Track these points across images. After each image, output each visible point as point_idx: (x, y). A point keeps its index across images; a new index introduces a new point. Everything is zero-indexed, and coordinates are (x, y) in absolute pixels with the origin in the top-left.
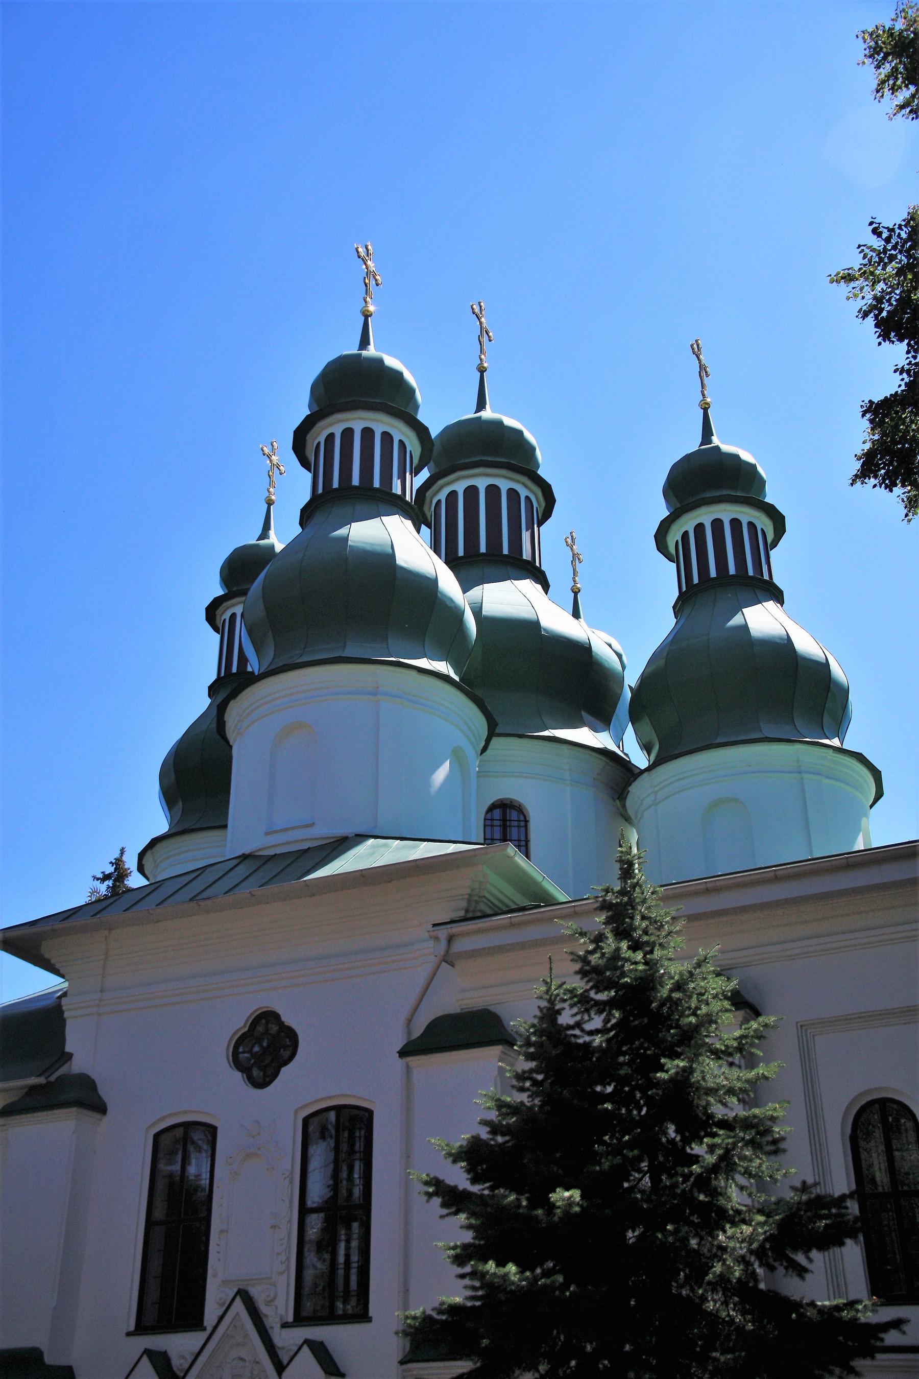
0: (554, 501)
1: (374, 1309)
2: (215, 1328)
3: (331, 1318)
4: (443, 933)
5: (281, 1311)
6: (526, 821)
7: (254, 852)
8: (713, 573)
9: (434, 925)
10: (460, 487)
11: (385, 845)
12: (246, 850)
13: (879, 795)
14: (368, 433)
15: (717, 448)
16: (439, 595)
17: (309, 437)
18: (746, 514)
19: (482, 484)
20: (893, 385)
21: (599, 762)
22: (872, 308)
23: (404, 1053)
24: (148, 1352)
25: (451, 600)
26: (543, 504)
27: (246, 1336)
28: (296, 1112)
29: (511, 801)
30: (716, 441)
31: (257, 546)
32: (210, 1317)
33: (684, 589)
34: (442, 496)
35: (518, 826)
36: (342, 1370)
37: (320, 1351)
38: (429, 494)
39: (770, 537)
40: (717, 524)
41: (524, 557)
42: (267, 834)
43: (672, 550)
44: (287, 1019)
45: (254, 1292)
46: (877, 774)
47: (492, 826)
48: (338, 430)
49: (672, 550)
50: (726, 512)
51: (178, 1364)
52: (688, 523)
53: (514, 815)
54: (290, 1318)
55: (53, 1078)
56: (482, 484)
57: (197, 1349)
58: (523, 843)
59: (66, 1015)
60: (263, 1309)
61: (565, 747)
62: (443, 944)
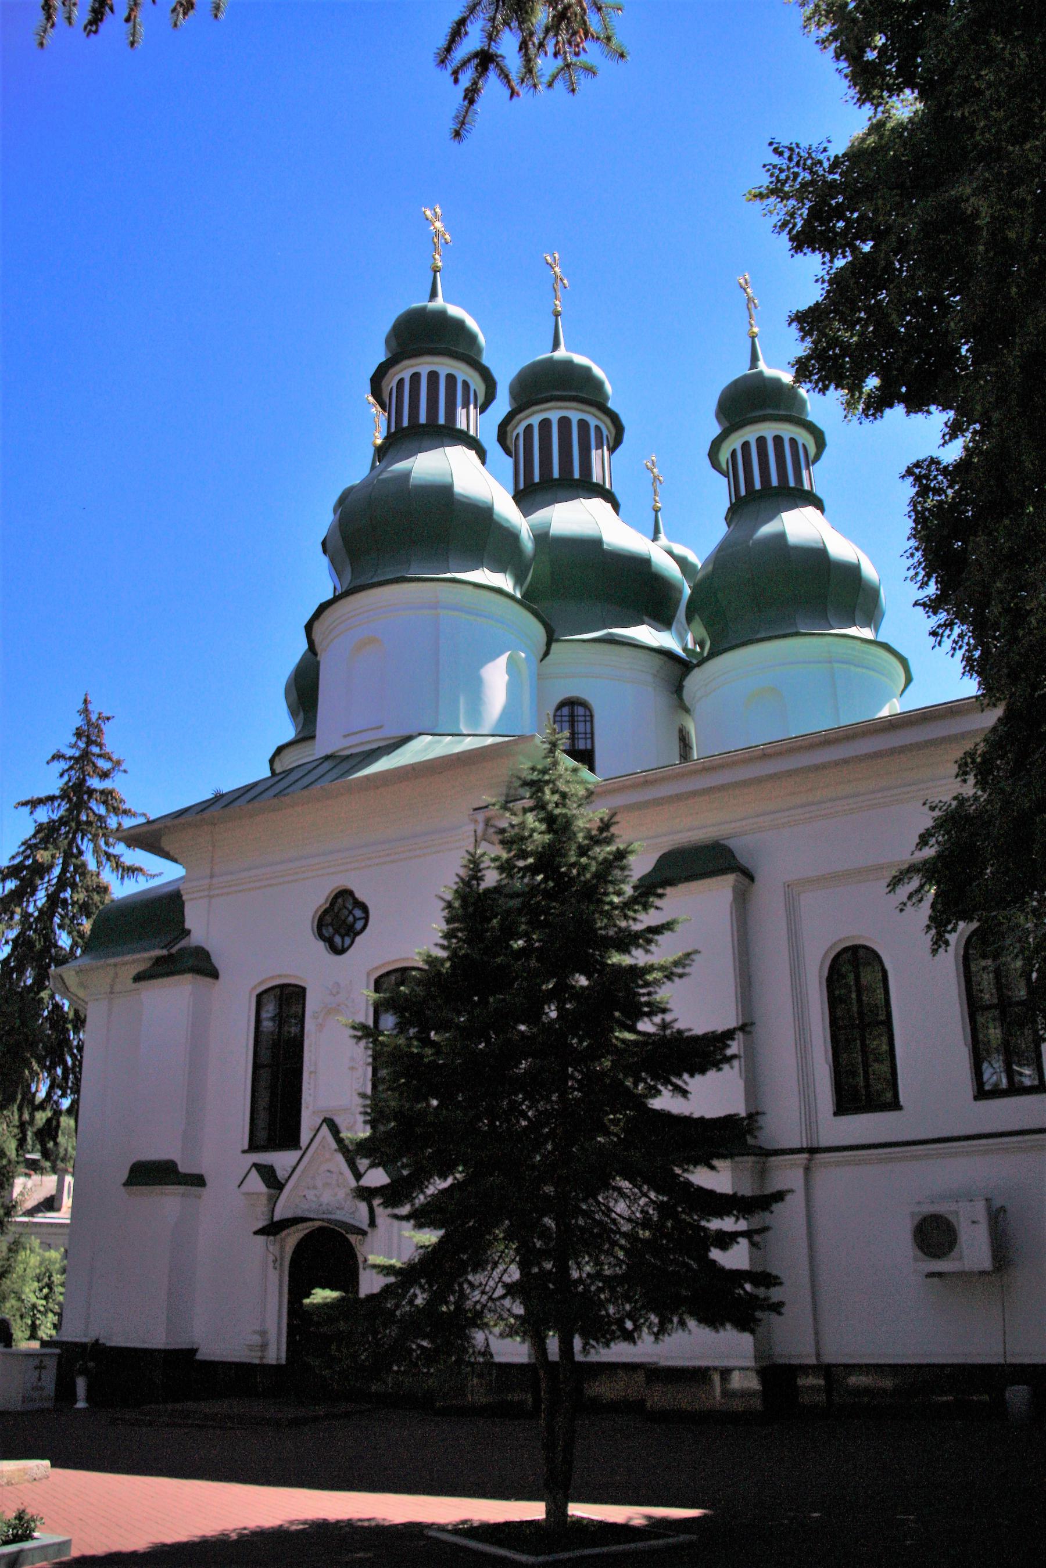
2: (307, 1148)
6: (592, 716)
7: (337, 751)
8: (758, 486)
9: (475, 809)
10: (535, 420)
11: (439, 742)
12: (329, 752)
13: (909, 680)
14: (433, 376)
15: (761, 373)
16: (495, 517)
17: (384, 383)
18: (788, 431)
19: (554, 416)
20: (813, 294)
21: (658, 660)
22: (785, 224)
24: (255, 1165)
25: (507, 521)
26: (613, 431)
28: (368, 974)
29: (578, 698)
30: (762, 366)
32: (305, 1137)
33: (734, 501)
34: (520, 430)
35: (585, 721)
38: (509, 428)
39: (812, 450)
40: (761, 441)
41: (595, 480)
42: (345, 736)
43: (724, 466)
45: (339, 1120)
46: (903, 661)
47: (561, 721)
48: (407, 375)
49: (724, 466)
50: (769, 430)
51: (281, 1174)
52: (735, 442)
53: (580, 711)
55: (174, 951)
56: (554, 416)
58: (589, 736)
59: (184, 898)
61: (624, 650)
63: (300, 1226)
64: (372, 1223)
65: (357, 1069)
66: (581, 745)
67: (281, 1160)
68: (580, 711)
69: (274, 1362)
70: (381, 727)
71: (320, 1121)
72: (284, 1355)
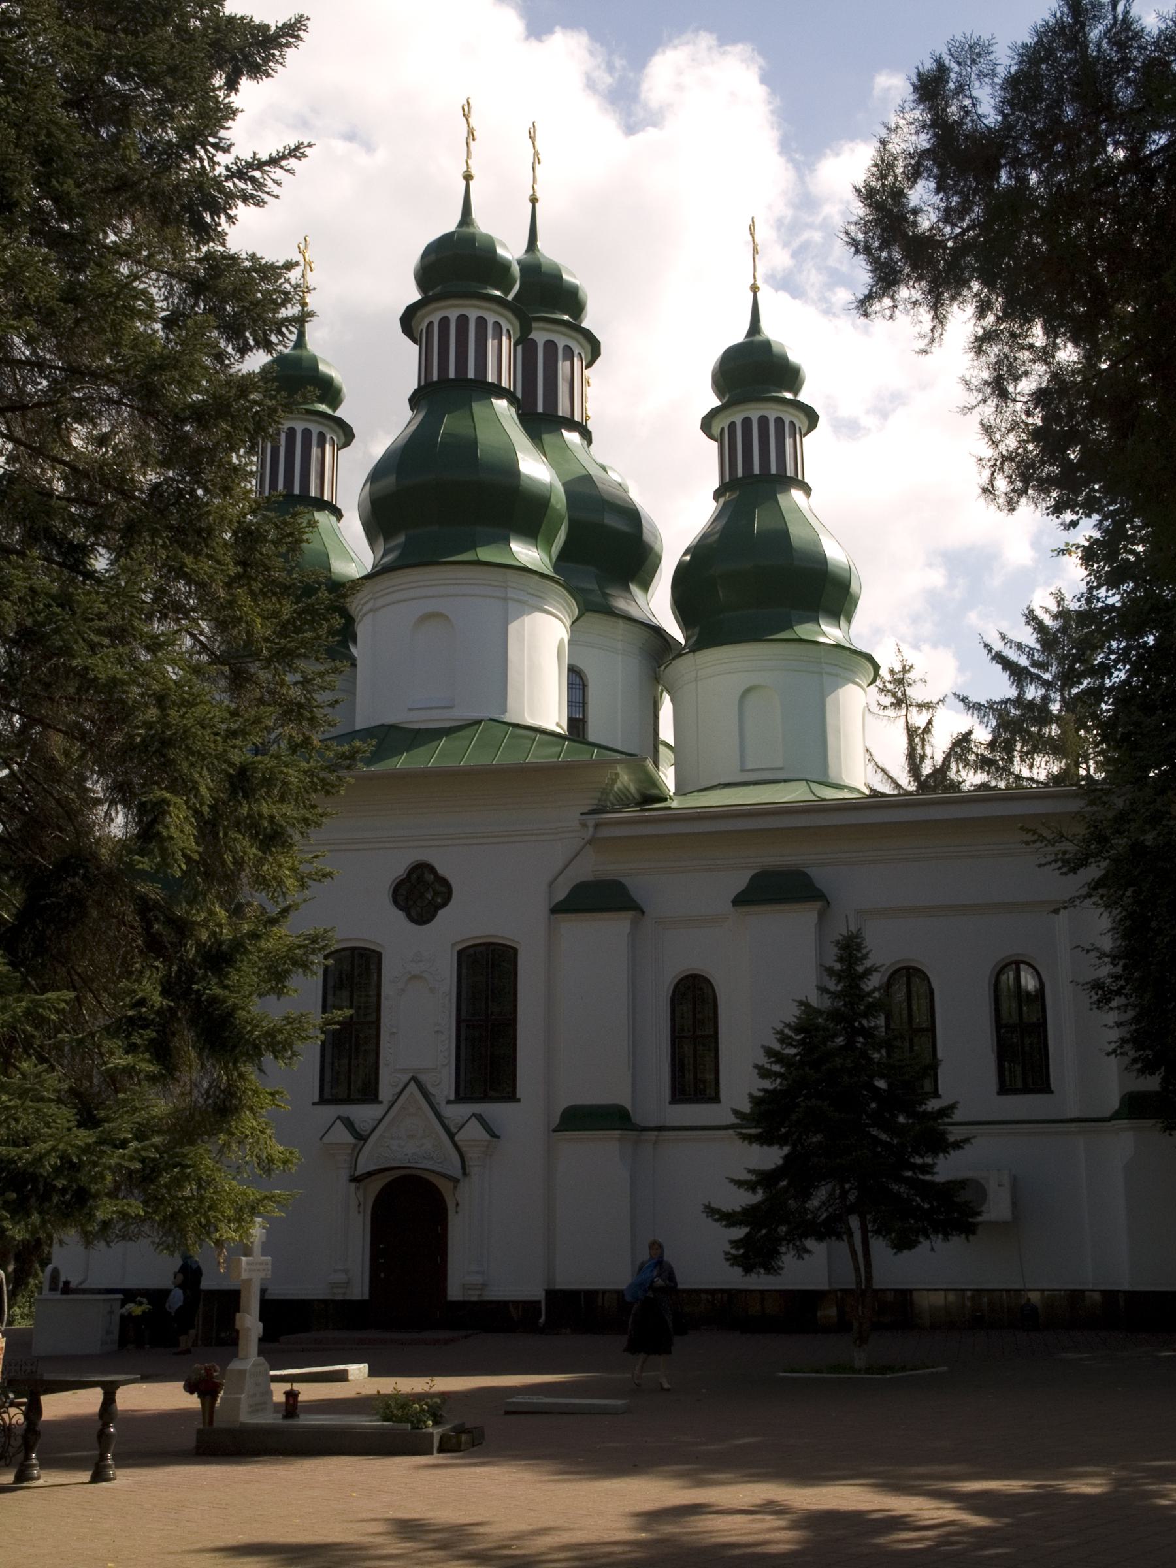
0: (599, 354)
1: (520, 1092)
3: (485, 1098)
4: (591, 820)
23: (558, 909)
24: (339, 1117)
32: (385, 1092)
36: (497, 1133)
37: (480, 1118)
42: (410, 709)
43: (716, 431)
44: (441, 871)
45: (423, 1078)
48: (453, 315)
51: (359, 1125)
52: (737, 416)
54: (452, 1097)
57: (380, 1117)
60: (431, 1090)
62: (591, 830)
63: (387, 1173)
64: (465, 1174)
65: (442, 1033)
67: (363, 1114)
69: (359, 1298)
71: (405, 1078)
72: (367, 1289)
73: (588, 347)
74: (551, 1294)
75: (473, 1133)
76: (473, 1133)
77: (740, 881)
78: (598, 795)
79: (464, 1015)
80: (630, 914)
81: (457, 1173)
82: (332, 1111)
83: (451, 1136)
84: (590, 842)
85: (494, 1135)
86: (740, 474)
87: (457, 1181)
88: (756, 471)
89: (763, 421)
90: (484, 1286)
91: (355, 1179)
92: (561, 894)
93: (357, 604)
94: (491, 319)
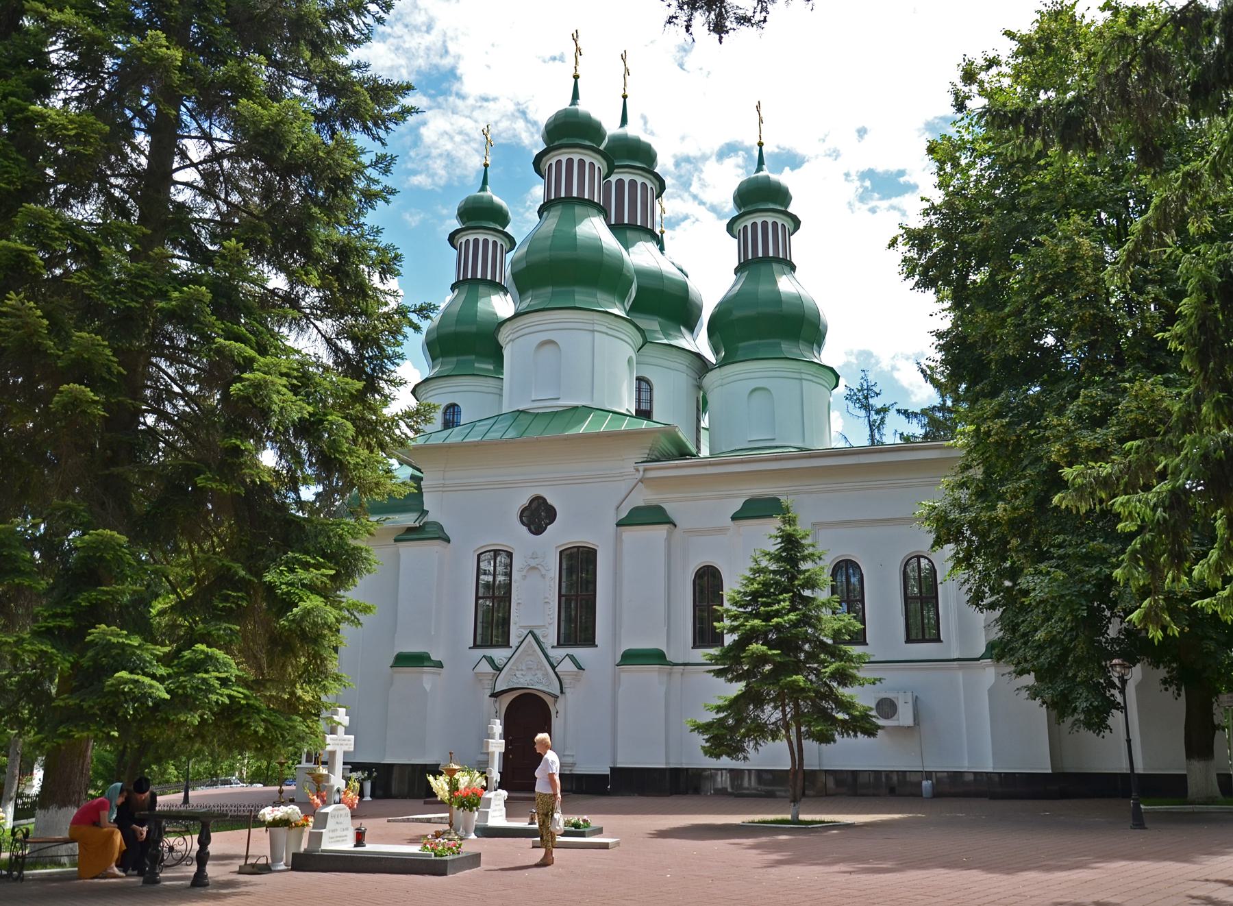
3: (576, 644)
4: (641, 467)
5: (551, 641)
6: (651, 390)
19: (627, 178)
23: (618, 525)
27: (535, 651)
31: (482, 197)
32: (514, 641)
37: (572, 658)
44: (550, 501)
45: (536, 632)
53: (644, 385)
60: (542, 639)
62: (641, 473)
64: (562, 692)
66: (644, 407)
67: (499, 654)
68: (644, 385)
70: (558, 399)
71: (526, 632)
73: (657, 183)
74: (612, 769)
75: (566, 667)
76: (566, 667)
77: (737, 505)
78: (648, 451)
79: (563, 592)
80: (666, 527)
81: (557, 692)
82: (481, 652)
83: (554, 668)
84: (641, 481)
85: (580, 668)
86: (750, 257)
87: (557, 697)
88: (760, 255)
89: (765, 224)
90: (574, 764)
91: (493, 695)
92: (623, 515)
93: (503, 337)
94: (588, 160)
